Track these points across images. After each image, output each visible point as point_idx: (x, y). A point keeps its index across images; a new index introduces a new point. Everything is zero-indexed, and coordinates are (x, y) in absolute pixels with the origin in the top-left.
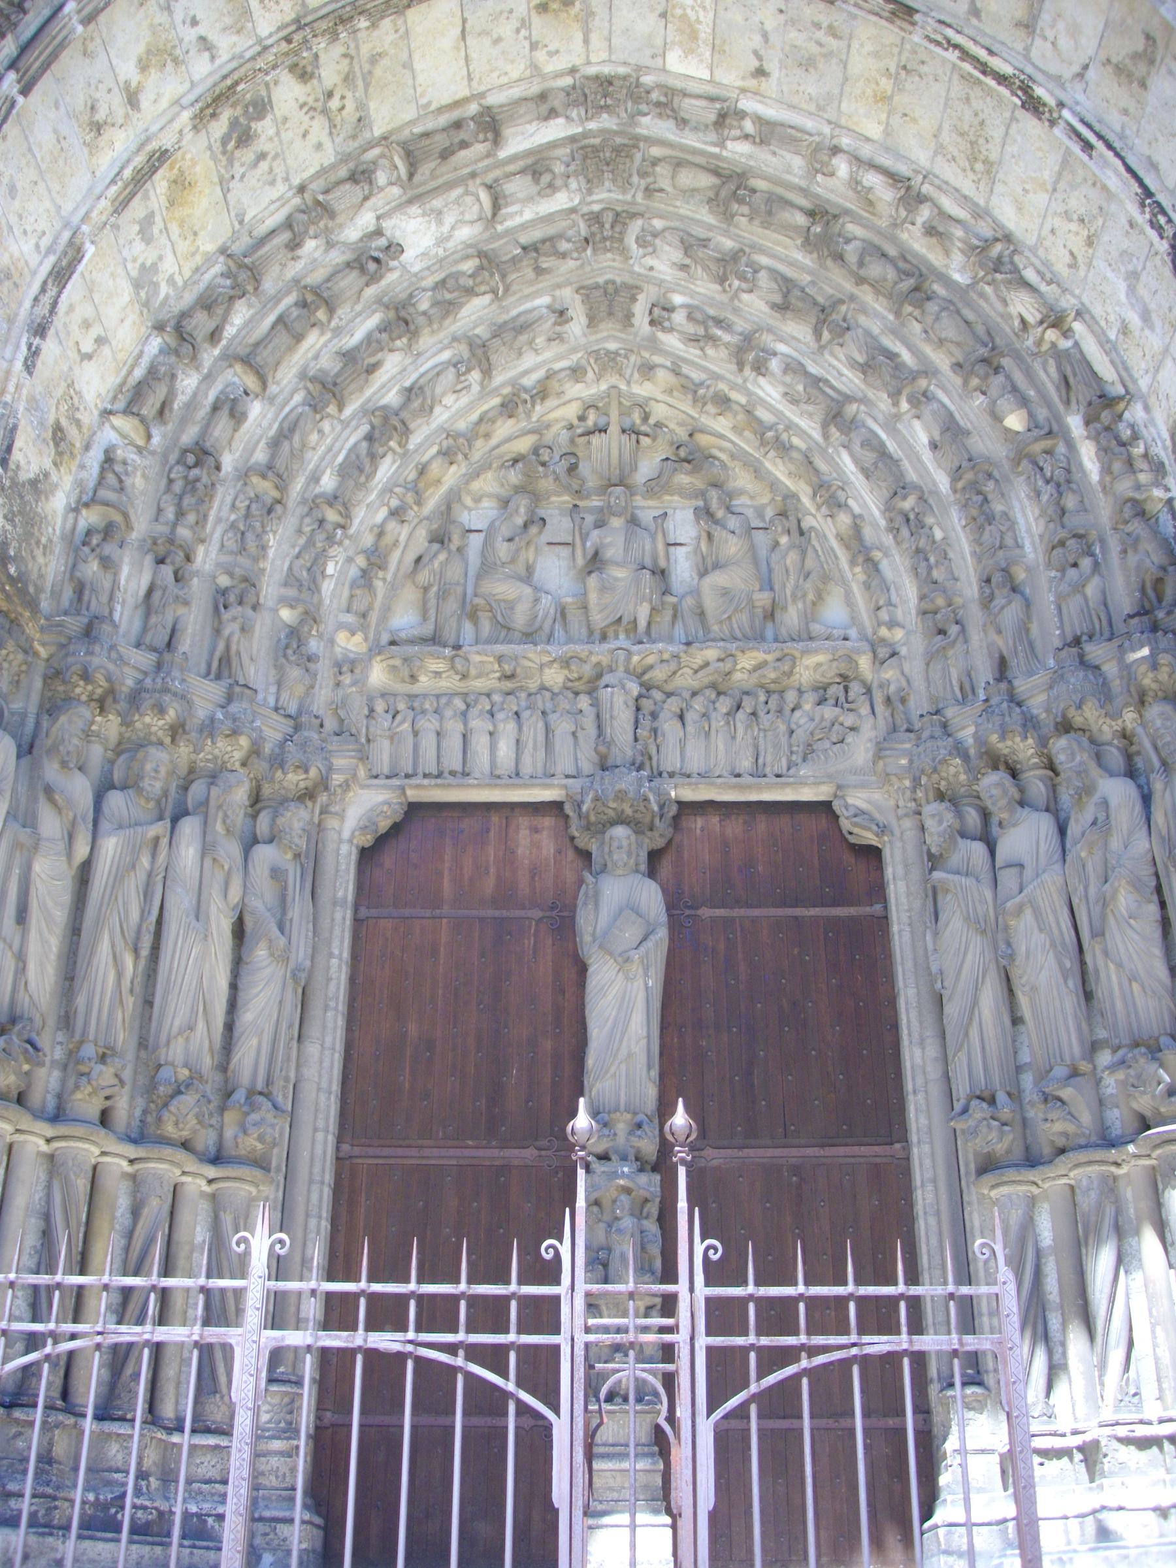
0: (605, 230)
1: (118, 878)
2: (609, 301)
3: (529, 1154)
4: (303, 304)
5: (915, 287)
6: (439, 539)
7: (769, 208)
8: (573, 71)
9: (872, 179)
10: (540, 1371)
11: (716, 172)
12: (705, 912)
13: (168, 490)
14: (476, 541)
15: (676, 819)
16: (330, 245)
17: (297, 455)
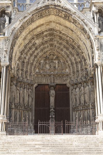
0: (51, 40)
1: (22, 94)
2: (52, 45)
3: (46, 108)
4: (30, 49)
5: (73, 48)
6: (39, 64)
7: (64, 40)
8: (49, 28)
9: (71, 39)
10: (49, 126)
11: (59, 36)
12: (58, 92)
13: (22, 65)
14: (42, 63)
15: (56, 86)
16: (31, 43)
17: (30, 60)
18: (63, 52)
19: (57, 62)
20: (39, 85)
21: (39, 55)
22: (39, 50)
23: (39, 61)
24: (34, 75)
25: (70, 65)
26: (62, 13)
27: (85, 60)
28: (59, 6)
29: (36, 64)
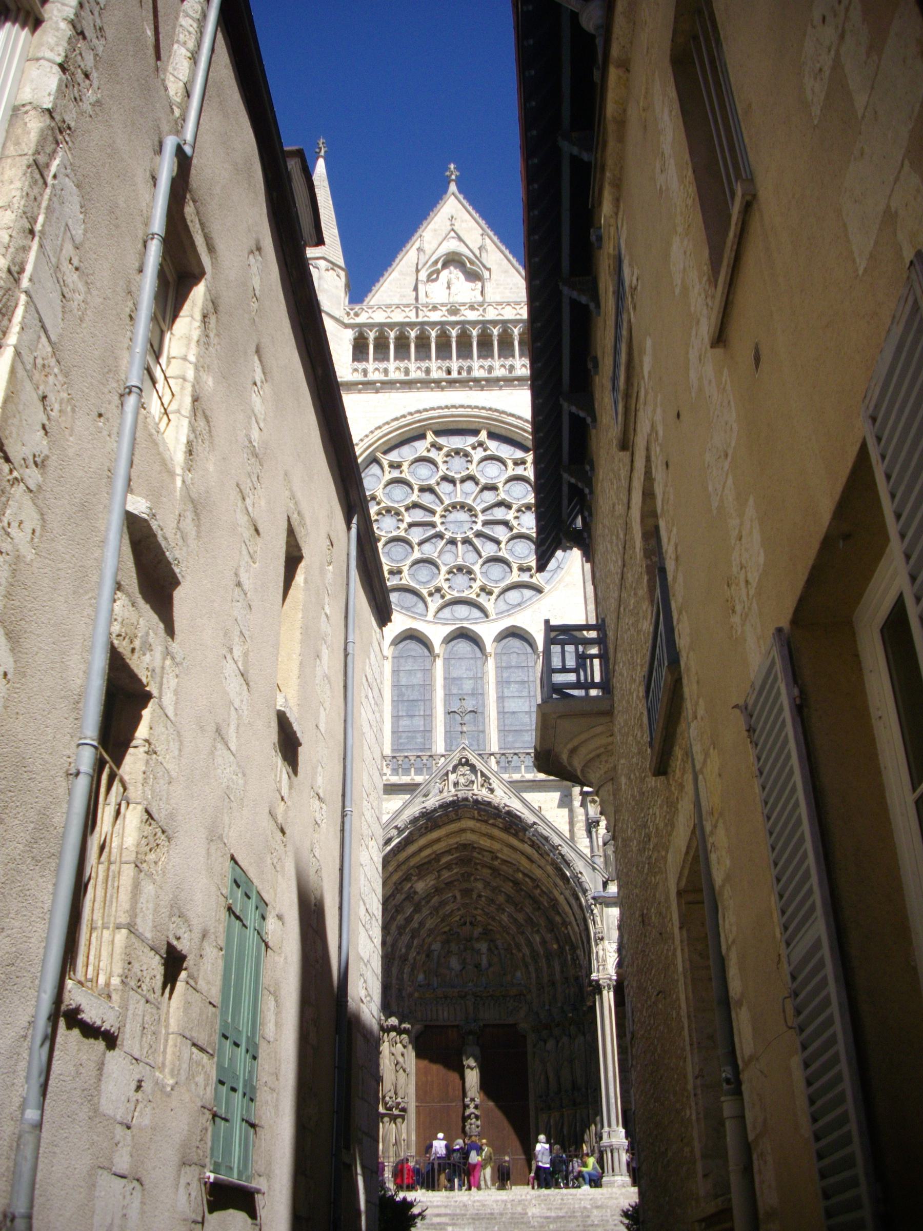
6: (428, 956)
9: (527, 879)
11: (490, 868)
14: (436, 953)
18: (503, 916)
19: (483, 947)
20: (426, 1027)
21: (427, 926)
22: (425, 912)
23: (425, 948)
24: (411, 995)
25: (529, 960)
26: (495, 819)
27: (574, 948)
28: (489, 803)
29: (418, 958)
